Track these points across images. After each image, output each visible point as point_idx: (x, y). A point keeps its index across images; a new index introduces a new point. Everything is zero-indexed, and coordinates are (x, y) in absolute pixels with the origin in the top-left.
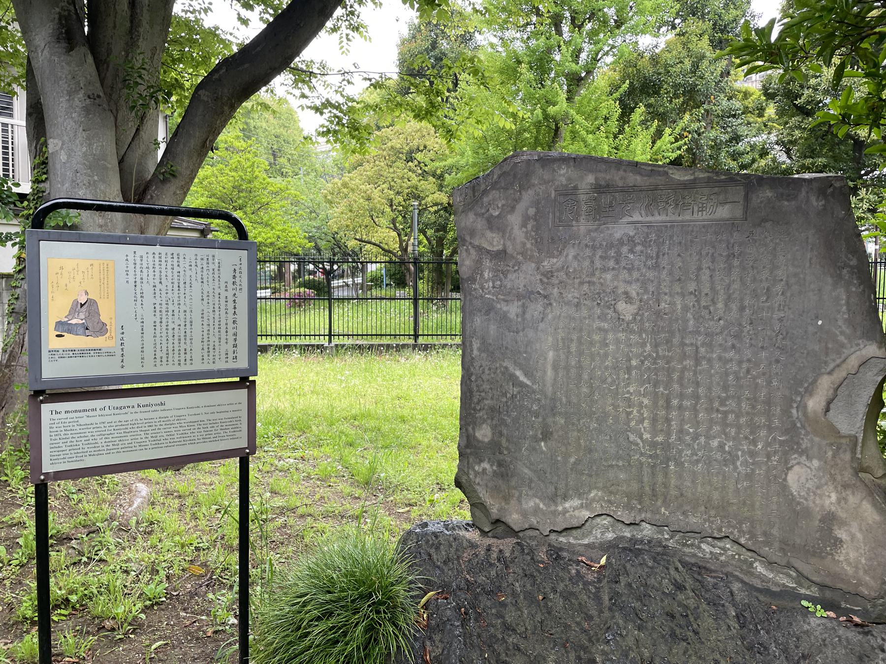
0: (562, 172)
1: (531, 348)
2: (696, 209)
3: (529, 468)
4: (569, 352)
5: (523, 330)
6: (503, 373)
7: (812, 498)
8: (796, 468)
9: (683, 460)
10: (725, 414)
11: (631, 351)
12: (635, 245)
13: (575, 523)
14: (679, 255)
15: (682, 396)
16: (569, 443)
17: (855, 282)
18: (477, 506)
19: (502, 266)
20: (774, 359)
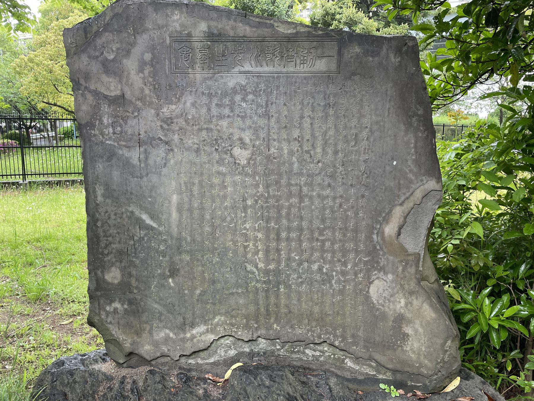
0: (176, 17)
1: (156, 192)
2: (298, 62)
3: (159, 303)
4: (192, 195)
5: (147, 175)
6: (129, 218)
7: (387, 304)
8: (376, 282)
9: (290, 283)
10: (323, 242)
11: (247, 192)
12: (247, 95)
13: (202, 346)
14: (285, 105)
15: (289, 229)
16: (195, 278)
17: (422, 128)
18: (110, 341)
19: (121, 112)
20: (360, 195)
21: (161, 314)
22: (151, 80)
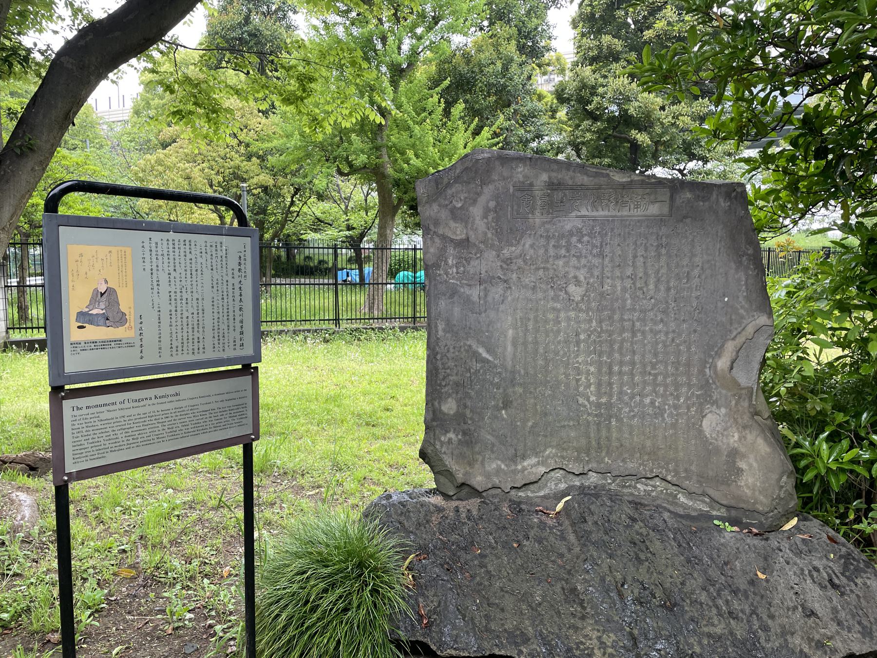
0: (519, 170)
2: (632, 206)
4: (527, 330)
6: (467, 351)
8: (709, 415)
10: (656, 375)
14: (619, 245)
15: (621, 363)
18: (440, 471)
21: (493, 445)
22: (493, 224)
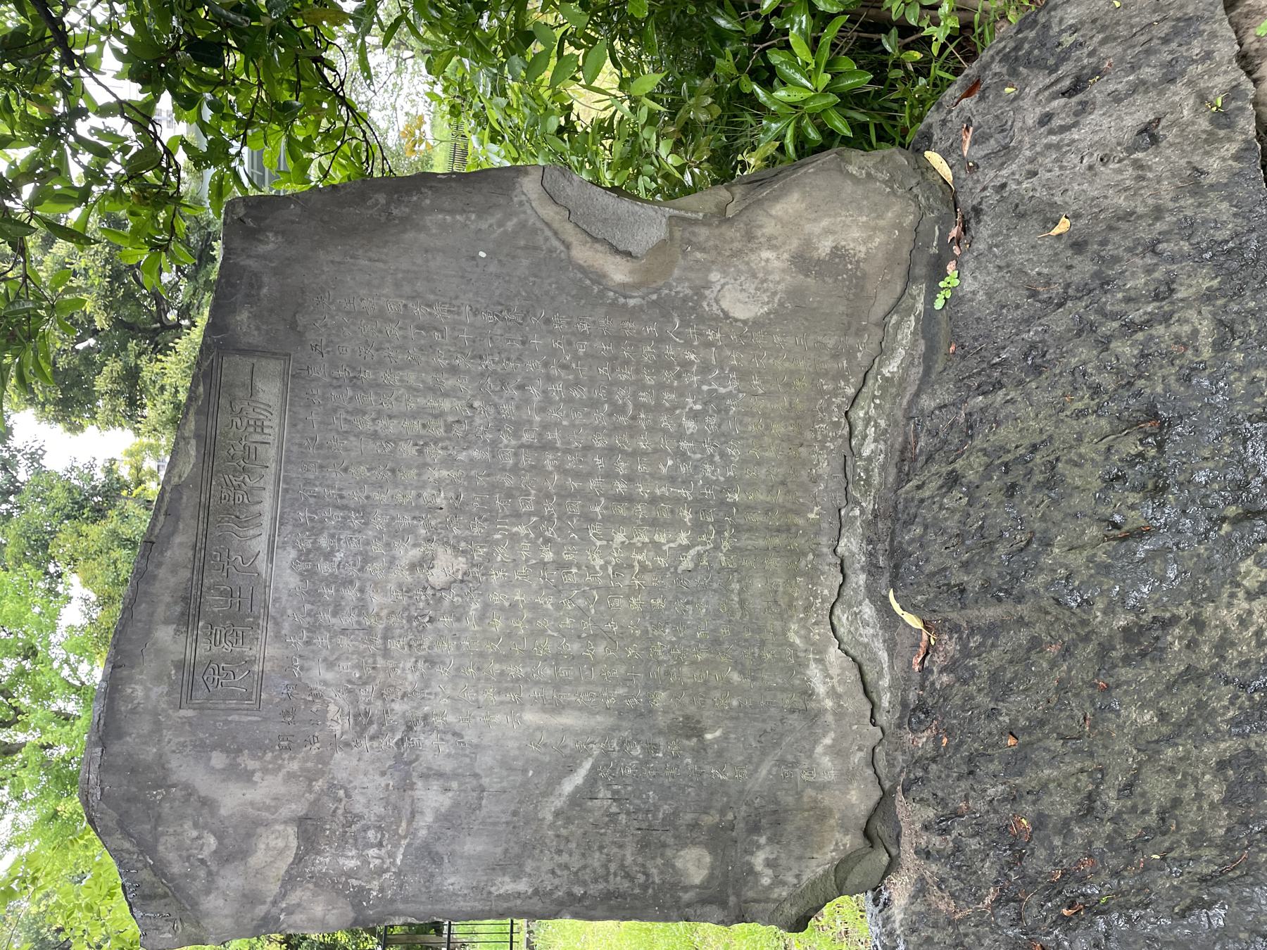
0: (140, 692)
1: (515, 758)
2: (258, 437)
3: (758, 766)
4: (526, 679)
5: (476, 776)
6: (569, 821)
7: (771, 285)
8: (725, 304)
9: (722, 479)
10: (638, 406)
11: (527, 560)
12: (319, 549)
13: (853, 675)
14: (346, 470)
16: (706, 682)
17: (415, 198)
19: (334, 826)
20: (544, 327)
21: (781, 762)
22: (269, 756)
